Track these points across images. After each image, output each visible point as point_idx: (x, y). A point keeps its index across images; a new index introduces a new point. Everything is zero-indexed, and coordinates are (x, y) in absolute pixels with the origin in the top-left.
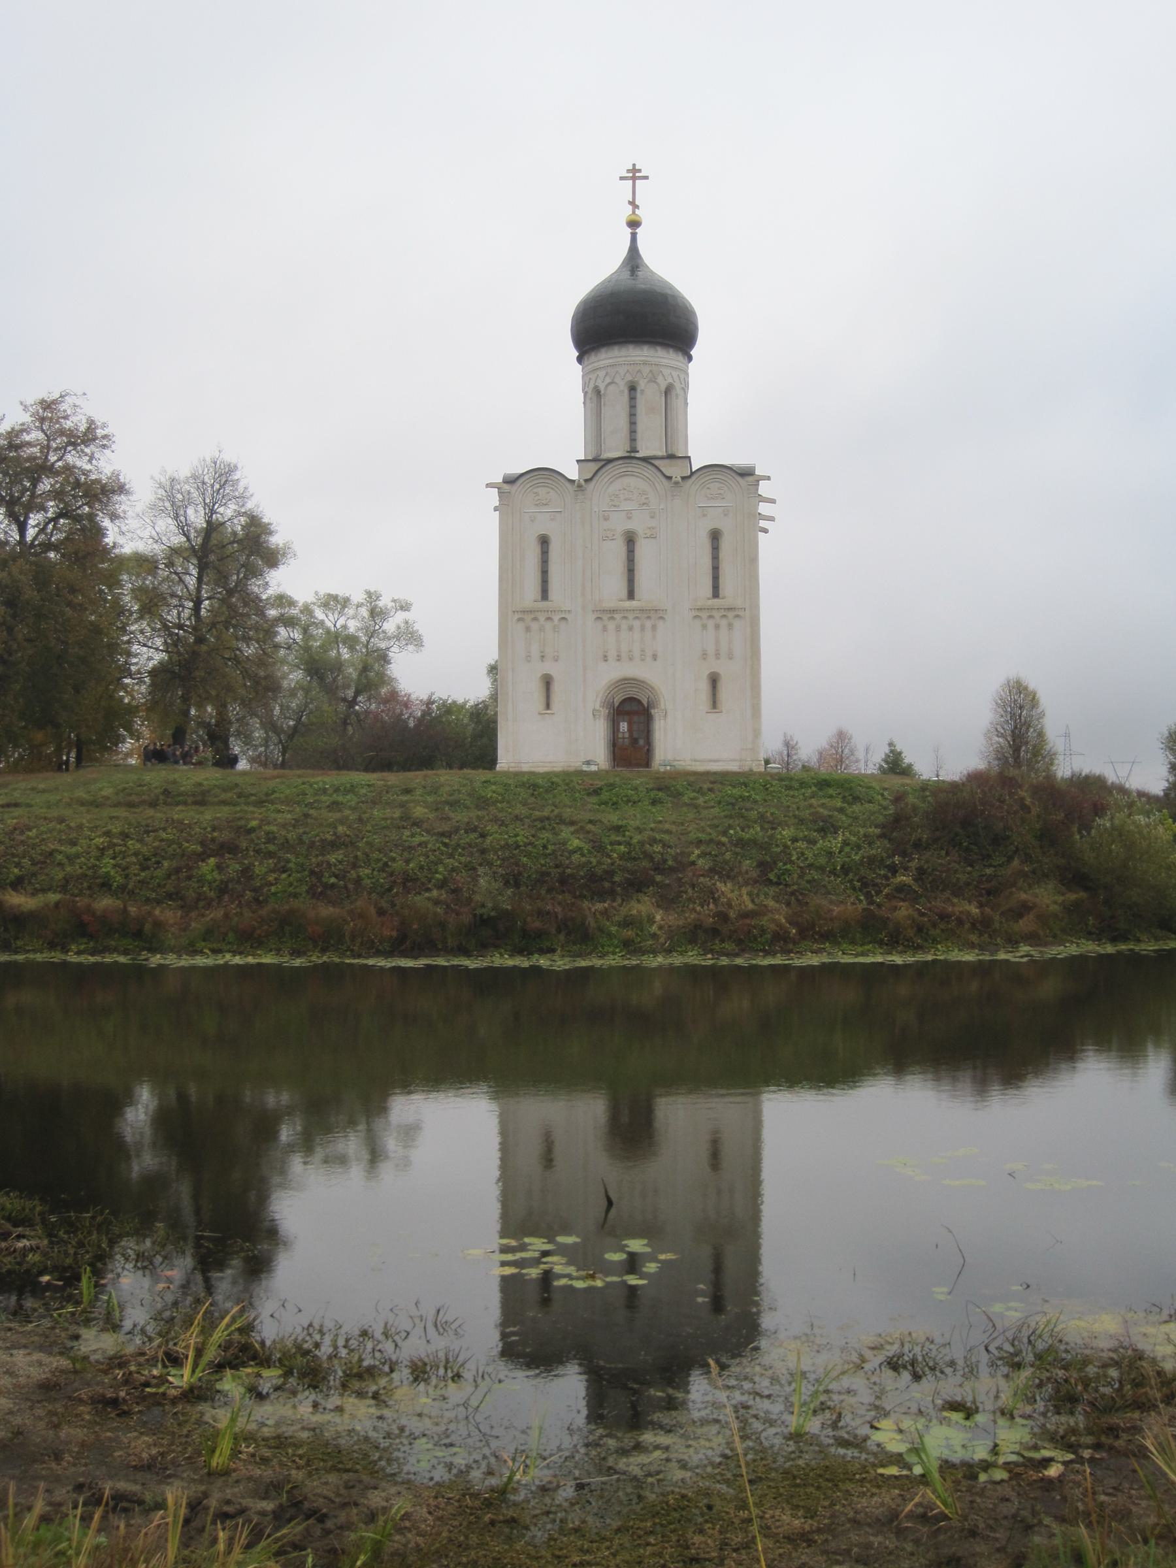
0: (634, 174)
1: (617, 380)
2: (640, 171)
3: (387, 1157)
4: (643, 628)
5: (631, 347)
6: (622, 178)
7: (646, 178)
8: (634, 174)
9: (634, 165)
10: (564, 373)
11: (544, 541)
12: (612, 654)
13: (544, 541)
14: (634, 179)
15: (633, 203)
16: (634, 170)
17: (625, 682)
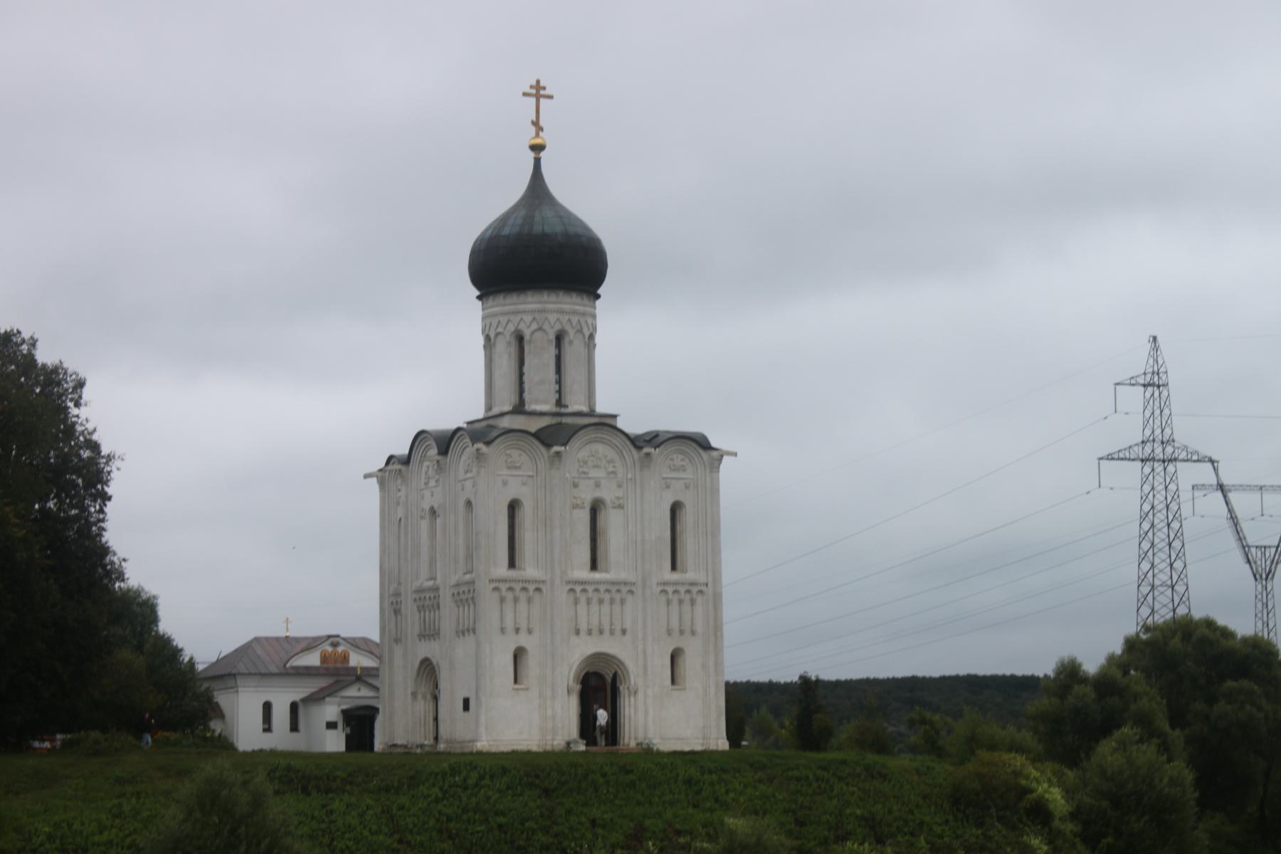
0: (538, 92)
1: (546, 327)
2: (544, 88)
4: (612, 601)
5: (561, 294)
6: (525, 94)
7: (550, 97)
8: (538, 92)
9: (538, 82)
11: (513, 507)
12: (583, 626)
13: (513, 507)
14: (538, 97)
15: (536, 123)
16: (538, 87)
17: (599, 657)
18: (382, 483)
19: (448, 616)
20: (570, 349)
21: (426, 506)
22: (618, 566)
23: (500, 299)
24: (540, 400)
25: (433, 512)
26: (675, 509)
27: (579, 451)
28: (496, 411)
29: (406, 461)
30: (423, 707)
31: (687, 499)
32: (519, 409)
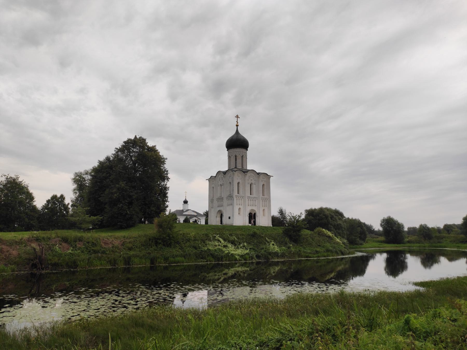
0: (237, 117)
3: (395, 277)
10: (225, 152)
15: (237, 122)
17: (252, 210)
18: (209, 181)
19: (225, 202)
20: (244, 158)
21: (219, 184)
22: (254, 195)
23: (230, 150)
24: (239, 166)
25: (221, 185)
26: (263, 185)
27: (249, 174)
28: (231, 168)
29: (215, 177)
30: (219, 219)
31: (265, 184)
32: (236, 168)
